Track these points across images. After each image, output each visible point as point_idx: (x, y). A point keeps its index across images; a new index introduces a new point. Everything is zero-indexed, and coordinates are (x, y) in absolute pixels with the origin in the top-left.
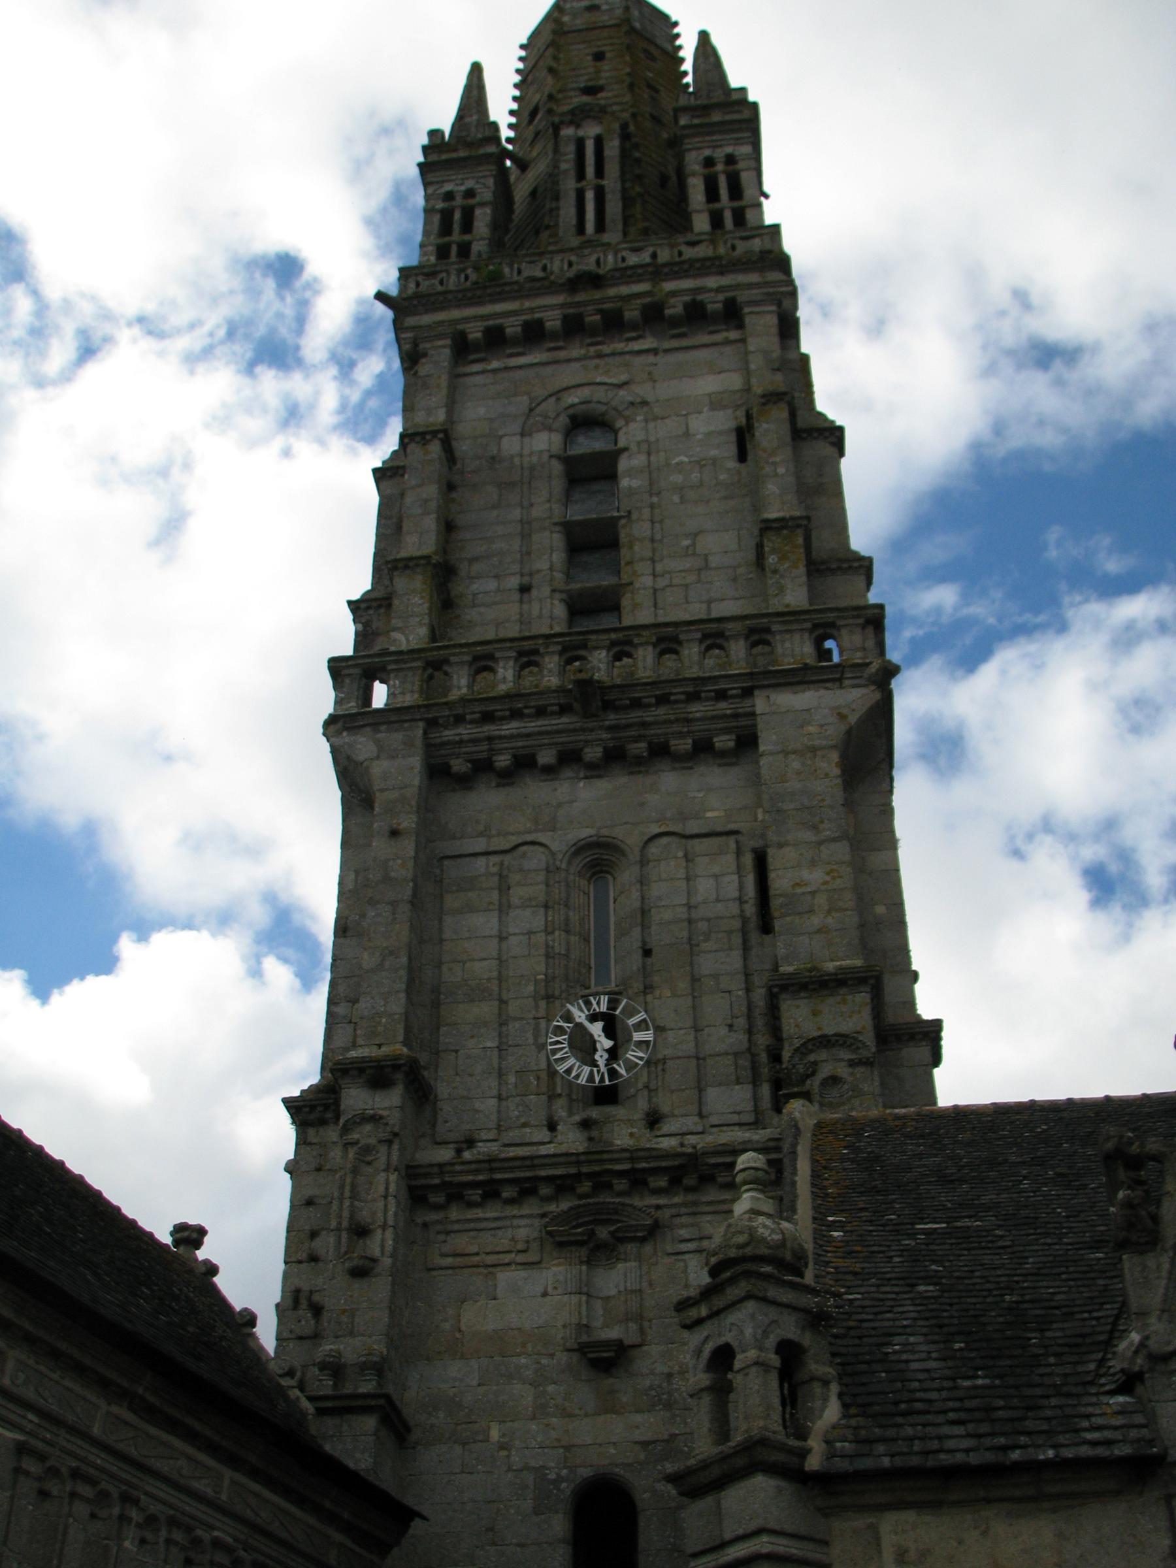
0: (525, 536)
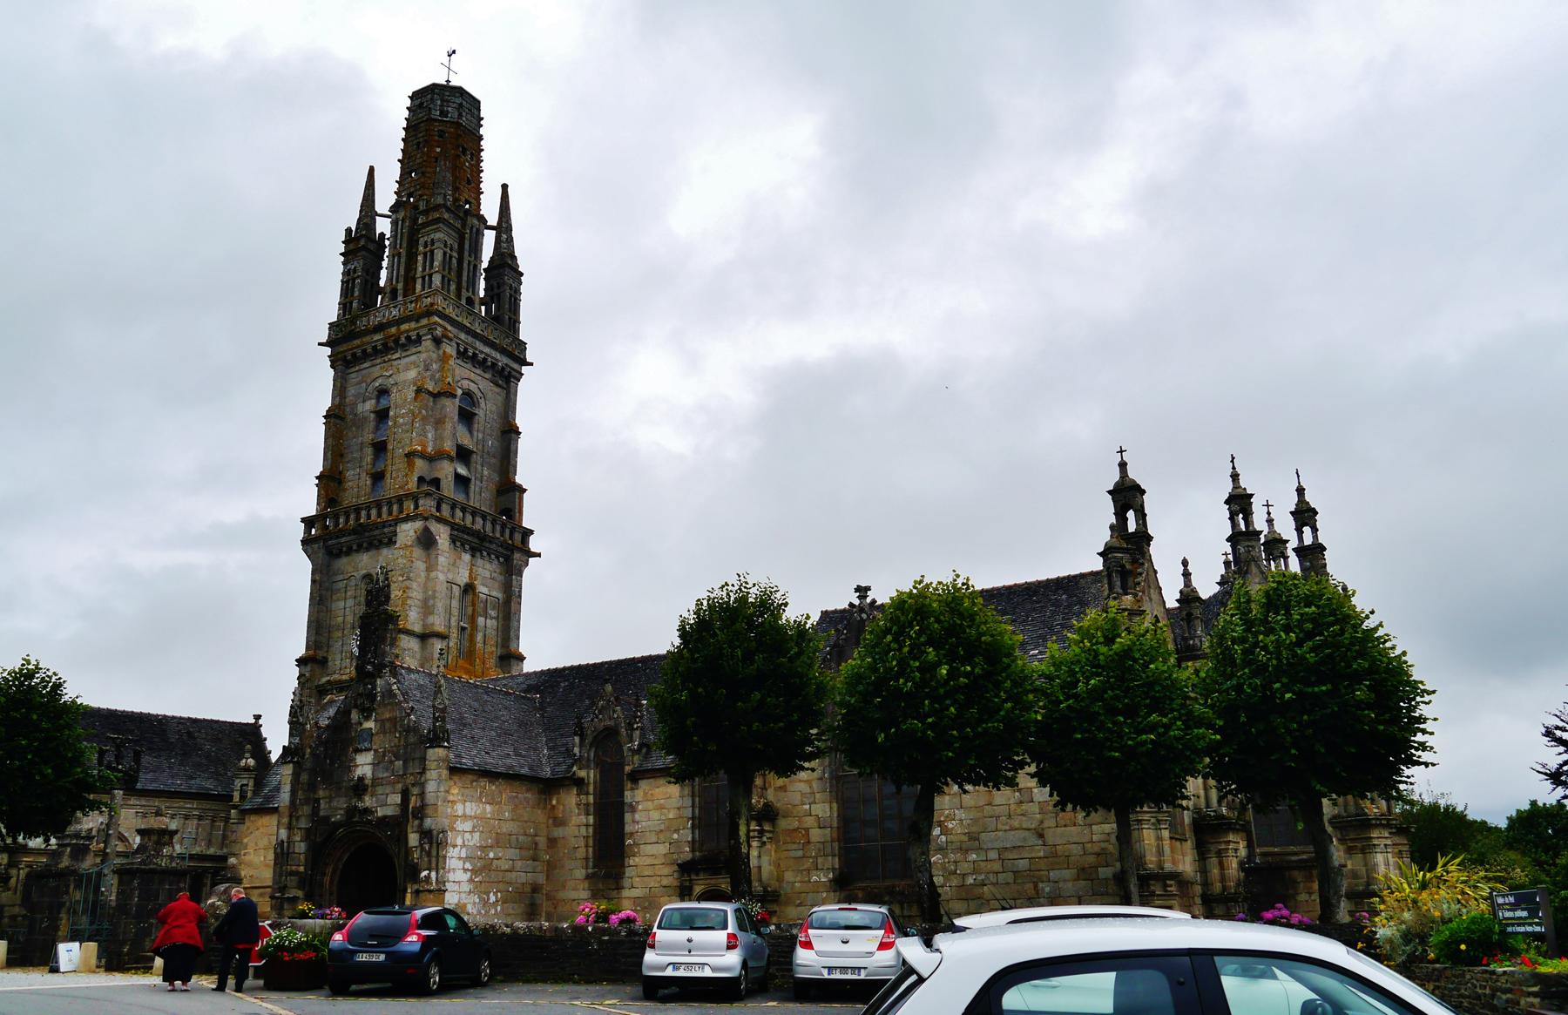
0: (361, 449)
